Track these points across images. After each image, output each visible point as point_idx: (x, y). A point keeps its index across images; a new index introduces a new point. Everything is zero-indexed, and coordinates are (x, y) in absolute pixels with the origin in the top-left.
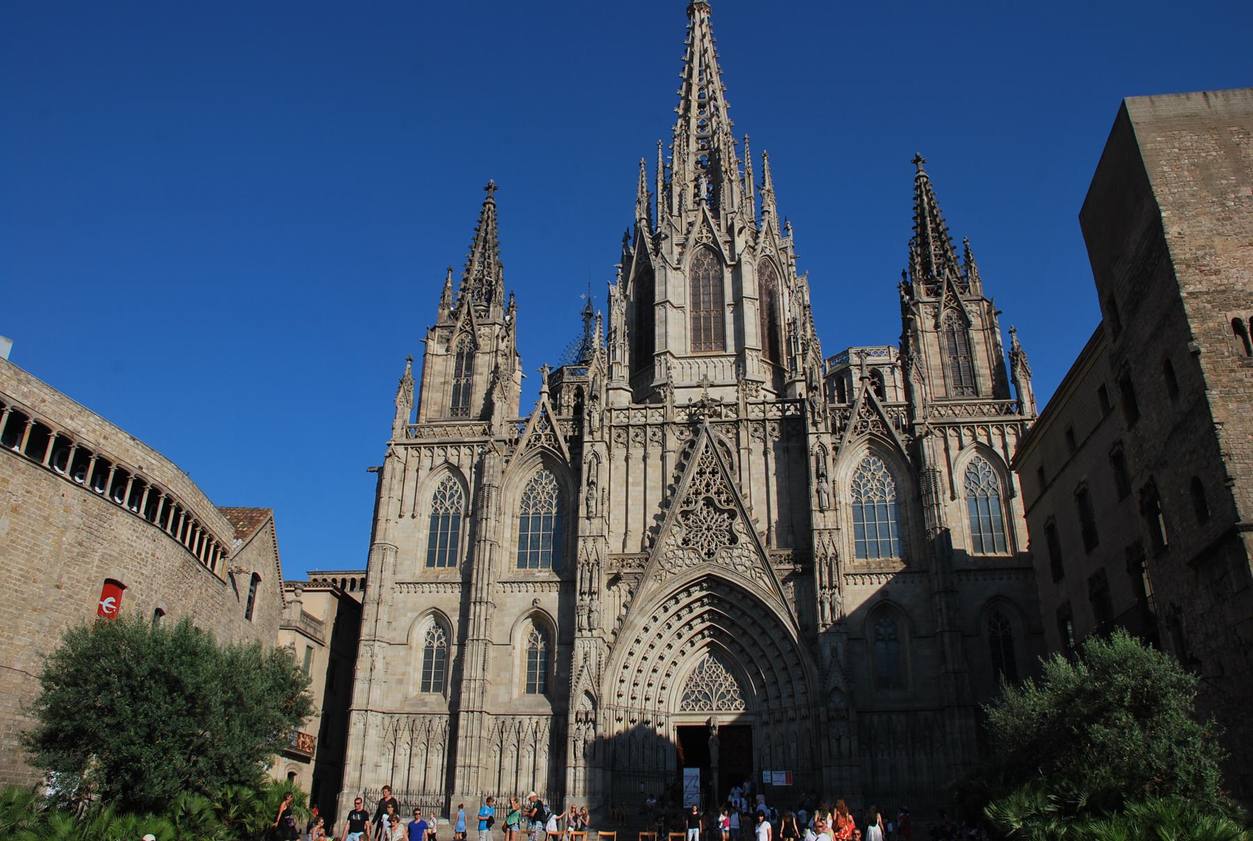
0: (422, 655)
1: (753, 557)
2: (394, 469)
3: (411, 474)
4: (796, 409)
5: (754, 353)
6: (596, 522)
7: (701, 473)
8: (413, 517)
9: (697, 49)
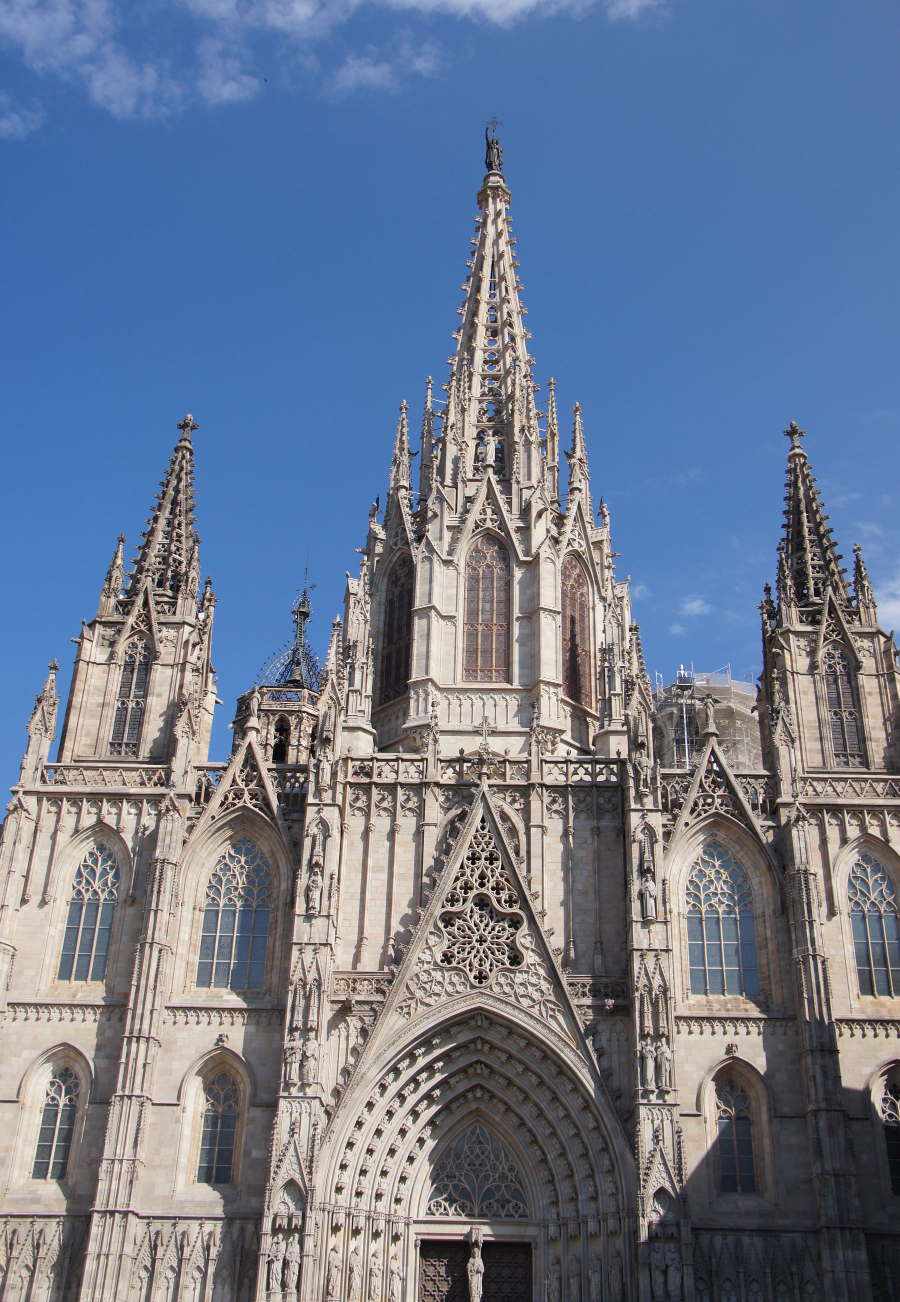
0: (38, 1119)
1: (544, 985)
2: (19, 829)
4: (612, 772)
5: (552, 690)
6: (319, 923)
7: (474, 858)
8: (43, 903)
9: (488, 251)
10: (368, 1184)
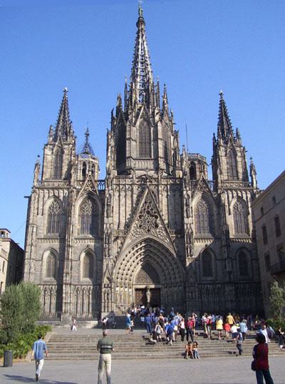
3: (41, 199)
7: (146, 202)
10: (123, 277)
